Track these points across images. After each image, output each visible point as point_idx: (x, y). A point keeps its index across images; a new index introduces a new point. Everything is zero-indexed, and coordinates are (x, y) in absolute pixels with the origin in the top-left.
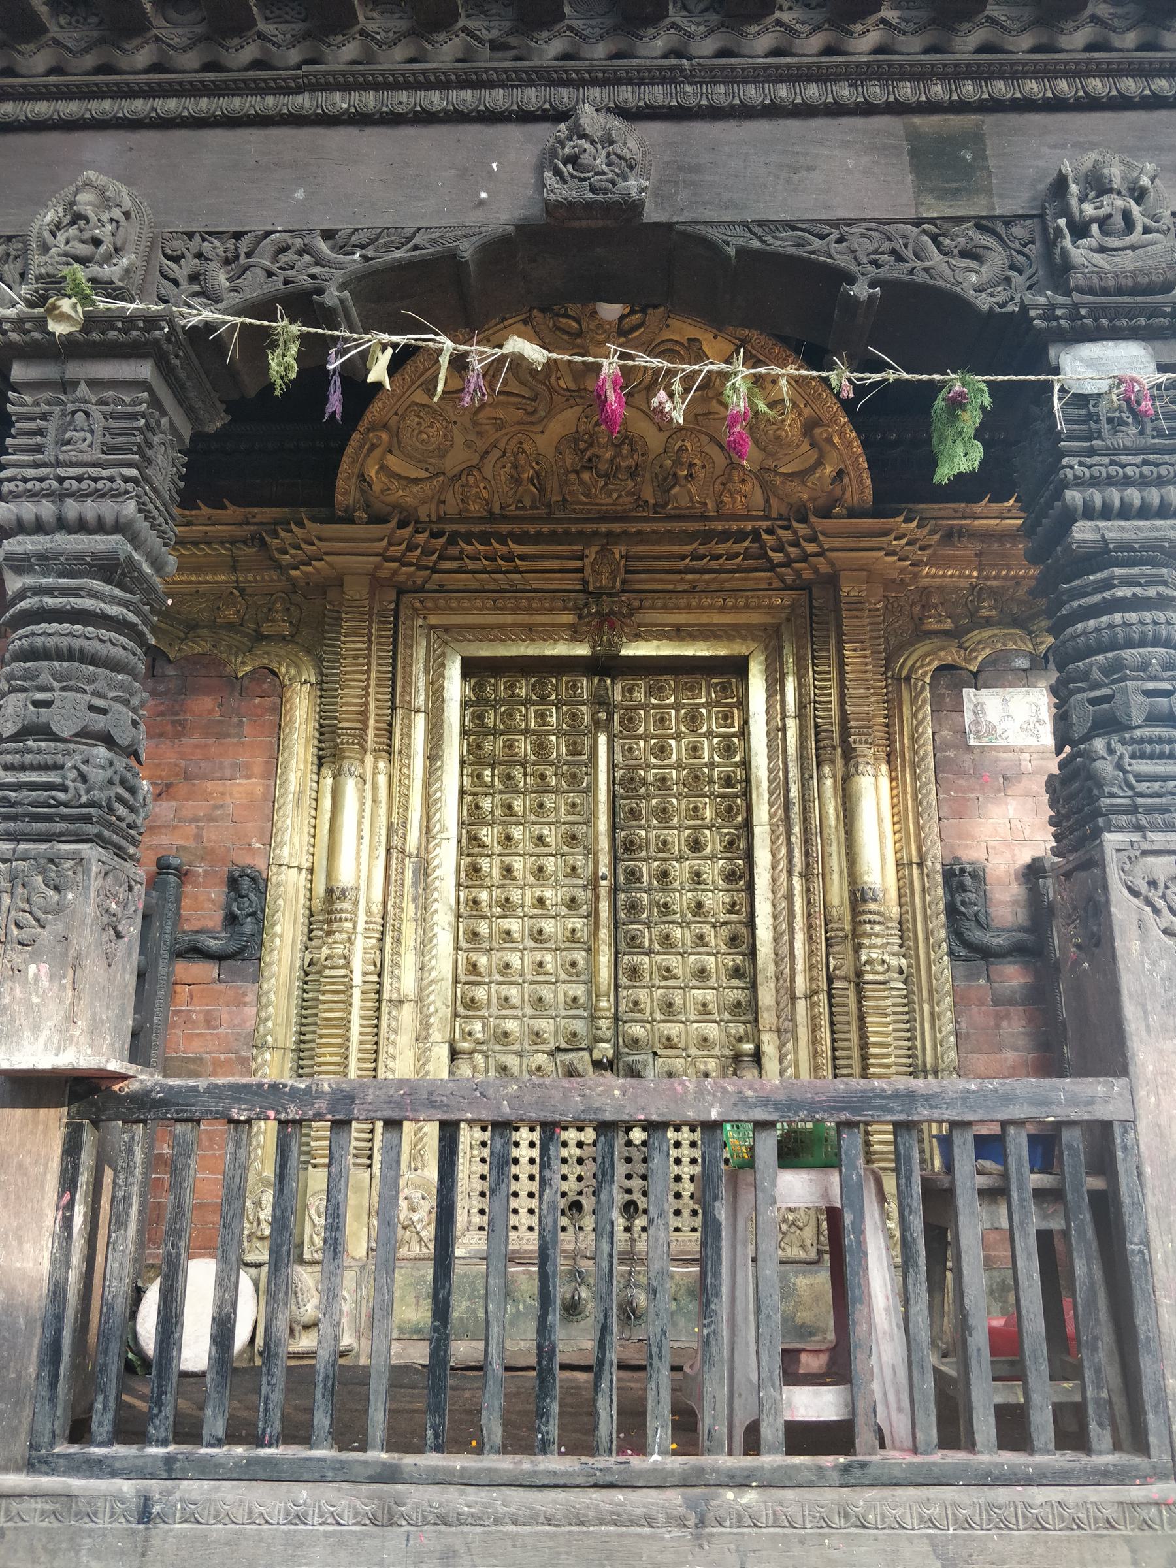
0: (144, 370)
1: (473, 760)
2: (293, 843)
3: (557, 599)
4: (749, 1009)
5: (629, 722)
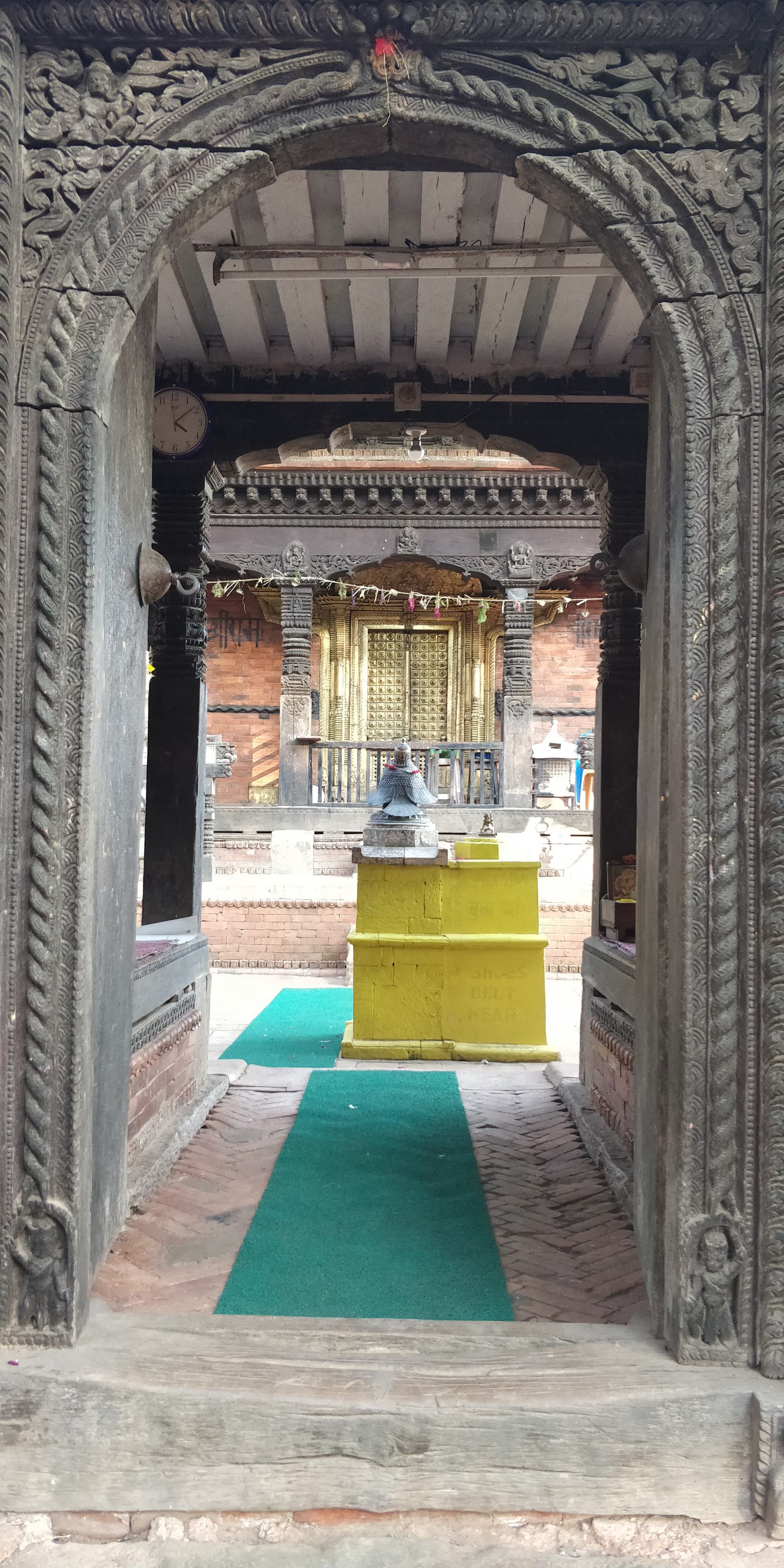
0: (310, 590)
1: (372, 657)
2: (326, 684)
3: (394, 614)
4: (444, 728)
5: (415, 648)
